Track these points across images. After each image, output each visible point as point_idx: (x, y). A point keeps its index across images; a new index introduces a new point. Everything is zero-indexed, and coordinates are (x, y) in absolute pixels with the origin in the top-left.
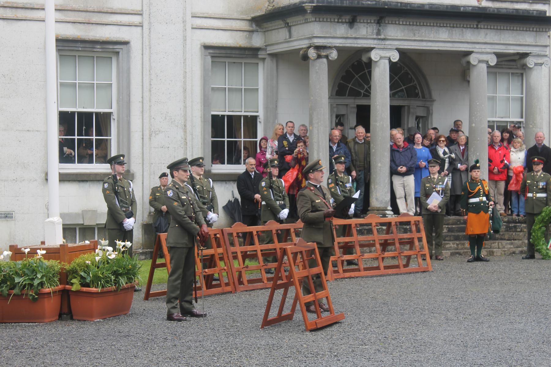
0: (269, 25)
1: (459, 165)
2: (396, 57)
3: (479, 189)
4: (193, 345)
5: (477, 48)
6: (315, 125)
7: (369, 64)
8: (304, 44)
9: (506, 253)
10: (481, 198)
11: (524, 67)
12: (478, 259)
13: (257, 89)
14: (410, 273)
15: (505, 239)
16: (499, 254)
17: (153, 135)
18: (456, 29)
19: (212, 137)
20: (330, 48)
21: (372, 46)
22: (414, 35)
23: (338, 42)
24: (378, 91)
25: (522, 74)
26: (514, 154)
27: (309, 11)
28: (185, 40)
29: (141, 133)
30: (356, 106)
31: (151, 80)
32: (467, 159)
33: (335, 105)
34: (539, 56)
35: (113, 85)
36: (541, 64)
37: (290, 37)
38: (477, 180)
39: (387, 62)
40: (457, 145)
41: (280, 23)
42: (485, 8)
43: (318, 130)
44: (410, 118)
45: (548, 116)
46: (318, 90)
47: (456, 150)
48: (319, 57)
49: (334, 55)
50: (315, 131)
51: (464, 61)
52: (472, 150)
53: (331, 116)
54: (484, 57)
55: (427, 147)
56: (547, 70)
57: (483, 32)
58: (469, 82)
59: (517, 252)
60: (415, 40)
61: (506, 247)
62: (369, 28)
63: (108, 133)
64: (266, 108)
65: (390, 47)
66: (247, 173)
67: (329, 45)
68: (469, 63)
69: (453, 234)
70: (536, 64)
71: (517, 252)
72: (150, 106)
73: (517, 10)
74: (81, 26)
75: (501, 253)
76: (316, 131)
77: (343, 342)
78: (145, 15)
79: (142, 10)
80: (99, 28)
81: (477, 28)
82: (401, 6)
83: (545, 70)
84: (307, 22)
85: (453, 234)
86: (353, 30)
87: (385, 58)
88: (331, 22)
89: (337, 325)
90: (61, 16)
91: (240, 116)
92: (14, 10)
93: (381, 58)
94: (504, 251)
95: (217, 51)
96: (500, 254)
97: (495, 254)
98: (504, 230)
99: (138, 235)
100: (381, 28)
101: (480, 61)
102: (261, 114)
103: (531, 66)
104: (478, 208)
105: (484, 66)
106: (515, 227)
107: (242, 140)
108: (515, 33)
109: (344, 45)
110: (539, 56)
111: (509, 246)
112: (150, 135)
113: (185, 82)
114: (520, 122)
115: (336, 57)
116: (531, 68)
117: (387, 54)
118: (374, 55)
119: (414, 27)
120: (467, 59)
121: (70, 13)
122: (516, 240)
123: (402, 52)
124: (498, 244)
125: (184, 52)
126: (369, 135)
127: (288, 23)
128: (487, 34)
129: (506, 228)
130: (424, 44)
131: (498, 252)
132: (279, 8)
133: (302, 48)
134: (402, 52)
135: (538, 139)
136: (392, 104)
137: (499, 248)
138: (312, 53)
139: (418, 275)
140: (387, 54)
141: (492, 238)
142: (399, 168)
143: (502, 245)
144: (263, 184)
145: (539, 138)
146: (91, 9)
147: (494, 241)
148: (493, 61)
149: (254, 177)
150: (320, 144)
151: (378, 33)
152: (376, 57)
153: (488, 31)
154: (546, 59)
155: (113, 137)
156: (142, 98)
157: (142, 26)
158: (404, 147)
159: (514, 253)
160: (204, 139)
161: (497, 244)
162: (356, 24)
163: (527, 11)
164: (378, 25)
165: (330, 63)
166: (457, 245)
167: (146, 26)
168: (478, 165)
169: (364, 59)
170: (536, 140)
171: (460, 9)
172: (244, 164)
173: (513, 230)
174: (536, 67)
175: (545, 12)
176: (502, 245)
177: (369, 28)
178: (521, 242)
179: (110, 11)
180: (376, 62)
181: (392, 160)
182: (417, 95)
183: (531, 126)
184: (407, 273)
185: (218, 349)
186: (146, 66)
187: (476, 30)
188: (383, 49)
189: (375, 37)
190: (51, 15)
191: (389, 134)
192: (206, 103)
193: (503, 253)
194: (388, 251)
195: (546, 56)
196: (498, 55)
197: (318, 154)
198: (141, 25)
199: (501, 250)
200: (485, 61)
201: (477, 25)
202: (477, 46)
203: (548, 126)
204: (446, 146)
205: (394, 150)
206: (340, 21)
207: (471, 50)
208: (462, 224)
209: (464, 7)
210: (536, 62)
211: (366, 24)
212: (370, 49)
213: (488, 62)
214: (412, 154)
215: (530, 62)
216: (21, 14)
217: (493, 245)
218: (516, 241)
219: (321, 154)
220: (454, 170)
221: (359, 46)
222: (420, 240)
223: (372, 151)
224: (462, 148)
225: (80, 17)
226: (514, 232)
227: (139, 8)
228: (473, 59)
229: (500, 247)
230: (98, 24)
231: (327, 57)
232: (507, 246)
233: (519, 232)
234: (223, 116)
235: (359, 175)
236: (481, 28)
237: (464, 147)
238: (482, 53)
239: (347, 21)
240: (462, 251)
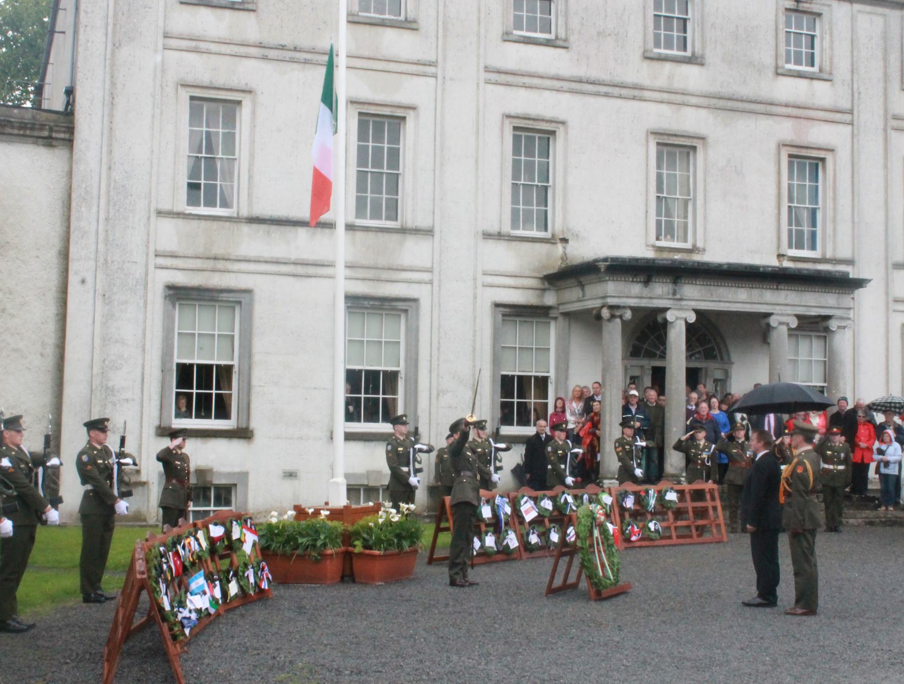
0: (561, 283)
2: (692, 318)
4: (474, 611)
5: (776, 309)
6: (608, 387)
7: (665, 324)
8: (597, 303)
11: (827, 329)
13: (549, 349)
14: (704, 543)
17: (441, 394)
18: (755, 290)
19: (502, 398)
20: (624, 307)
21: (668, 306)
22: (712, 295)
23: (633, 302)
25: (825, 337)
27: (602, 270)
28: (475, 298)
29: (428, 393)
30: (650, 367)
31: (439, 338)
33: (629, 367)
34: (842, 318)
35: (401, 344)
36: (844, 327)
37: (583, 296)
39: (683, 323)
41: (571, 282)
42: (786, 269)
43: (611, 392)
44: (708, 380)
48: (613, 316)
49: (628, 315)
51: (763, 322)
53: (625, 377)
54: (785, 319)
55: (724, 411)
56: (851, 333)
57: (783, 294)
58: (769, 344)
60: (712, 301)
62: (664, 288)
63: (394, 391)
64: (557, 368)
65: (686, 307)
66: (538, 435)
67: (622, 305)
68: (768, 325)
70: (839, 327)
72: (438, 365)
73: (819, 271)
74: (371, 283)
77: (628, 612)
78: (436, 272)
79: (432, 267)
80: (388, 284)
81: (777, 289)
82: (698, 265)
83: (848, 333)
84: (601, 281)
86: (647, 289)
87: (681, 318)
88: (625, 281)
89: (624, 595)
90: (350, 273)
91: (530, 377)
92: (304, 266)
93: (677, 318)
95: (507, 310)
99: (421, 495)
100: (676, 288)
101: (781, 323)
102: (552, 374)
103: (834, 329)
107: (533, 401)
108: (817, 295)
109: (639, 305)
110: (842, 318)
112: (438, 395)
113: (474, 341)
114: (823, 387)
116: (833, 331)
117: (683, 314)
118: (670, 316)
119: (712, 288)
120: (766, 321)
121: (360, 270)
123: (698, 312)
125: (474, 310)
126: (662, 398)
127: (581, 282)
128: (787, 296)
130: (722, 304)
132: (572, 266)
133: (595, 308)
134: (698, 312)
138: (605, 313)
139: (712, 546)
140: (683, 314)
144: (549, 449)
146: (381, 266)
148: (794, 323)
149: (545, 439)
151: (674, 293)
153: (789, 293)
155: (400, 397)
156: (431, 356)
157: (432, 284)
160: (493, 400)
162: (651, 283)
163: (829, 272)
164: (674, 285)
165: (624, 323)
167: (436, 283)
169: (660, 319)
171: (759, 270)
172: (535, 425)
174: (839, 330)
175: (848, 274)
177: (664, 288)
179: (400, 268)
180: (672, 323)
182: (714, 357)
184: (699, 543)
185: (500, 616)
186: (435, 324)
187: (776, 292)
188: (680, 309)
189: (671, 296)
190: (341, 271)
192: (496, 361)
194: (682, 520)
195: (849, 319)
196: (799, 317)
197: (610, 417)
198: (431, 282)
201: (777, 286)
202: (778, 308)
206: (635, 280)
207: (771, 311)
209: (764, 267)
211: (660, 284)
212: (665, 310)
215: (833, 325)
216: (311, 270)
219: (613, 417)
221: (654, 306)
222: (715, 508)
223: (667, 415)
225: (370, 274)
227: (429, 265)
228: (773, 321)
230: (387, 281)
231: (621, 317)
234: (513, 376)
236: (781, 289)
238: (782, 315)
239: (642, 280)
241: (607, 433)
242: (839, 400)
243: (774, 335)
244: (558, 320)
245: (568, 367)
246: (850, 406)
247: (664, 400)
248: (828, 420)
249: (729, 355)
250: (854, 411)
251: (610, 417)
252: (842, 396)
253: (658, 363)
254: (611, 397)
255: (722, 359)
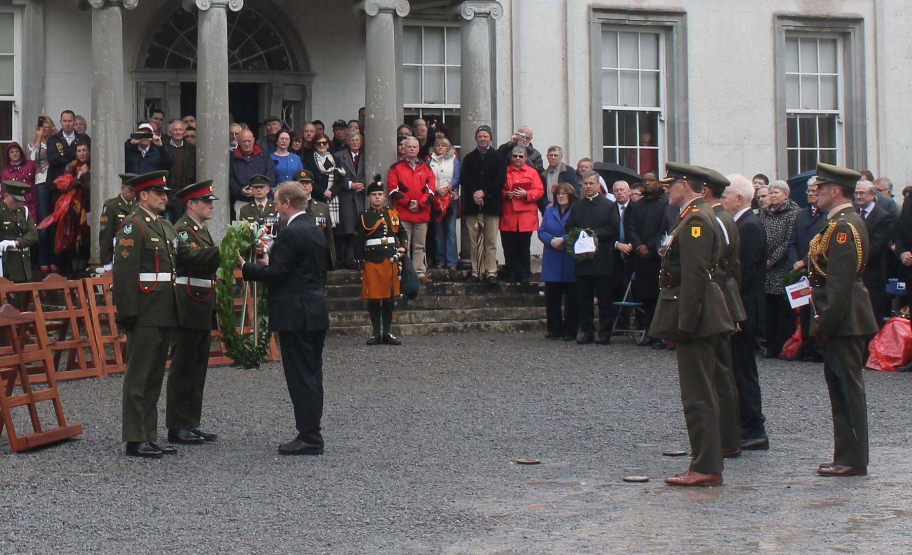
1: (350, 183)
3: (382, 224)
6: (101, 118)
9: (421, 330)
10: (384, 239)
11: (458, 18)
12: (387, 341)
15: (423, 308)
16: (409, 333)
24: (208, 60)
26: (436, 164)
32: (363, 174)
38: (379, 208)
39: (223, 11)
40: (347, 149)
45: (510, 100)
46: (105, 60)
47: (344, 159)
50: (101, 128)
52: (370, 157)
59: (441, 329)
61: (423, 321)
68: (363, 12)
69: (335, 299)
70: (477, 15)
71: (441, 329)
75: (413, 331)
76: (103, 128)
85: (335, 299)
94: (419, 327)
96: (411, 333)
97: (402, 333)
98: (423, 292)
103: (469, 18)
104: (381, 253)
105: (389, 17)
106: (443, 287)
111: (429, 320)
115: (136, 5)
122: (441, 309)
124: (410, 316)
129: (427, 288)
131: (408, 329)
135: (480, 139)
136: (231, 81)
137: (411, 323)
141: (404, 306)
142: (244, 190)
143: (416, 317)
145: (483, 139)
147: (404, 312)
150: (110, 149)
152: (204, 4)
154: (495, 5)
158: (253, 153)
159: (435, 330)
161: (407, 316)
166: (340, 317)
168: (379, 183)
170: (478, 142)
173: (439, 292)
176: (416, 317)
178: (448, 312)
181: (233, 175)
183: (470, 118)
191: (228, 132)
193: (416, 331)
197: (106, 165)
199: (414, 326)
200: (390, 9)
203: (510, 116)
204: (328, 150)
205: (237, 159)
208: (353, 282)
210: (476, 11)
213: (395, 11)
214: (266, 165)
217: (401, 317)
218: (440, 311)
220: (340, 188)
224: (354, 155)
226: (440, 295)
229: (413, 320)
232: (426, 319)
233: (450, 295)
235: (175, 201)
237: (357, 154)
240: (346, 328)
241: (101, 191)
242: (478, 131)
243: (373, 31)
244: (26, 10)
245: (43, 86)
246: (503, 138)
247: (193, 136)
248: (461, 162)
249: (307, 62)
250: (508, 148)
251: (106, 165)
252: (483, 124)
253: (186, 78)
254: (106, 132)
255: (296, 68)
